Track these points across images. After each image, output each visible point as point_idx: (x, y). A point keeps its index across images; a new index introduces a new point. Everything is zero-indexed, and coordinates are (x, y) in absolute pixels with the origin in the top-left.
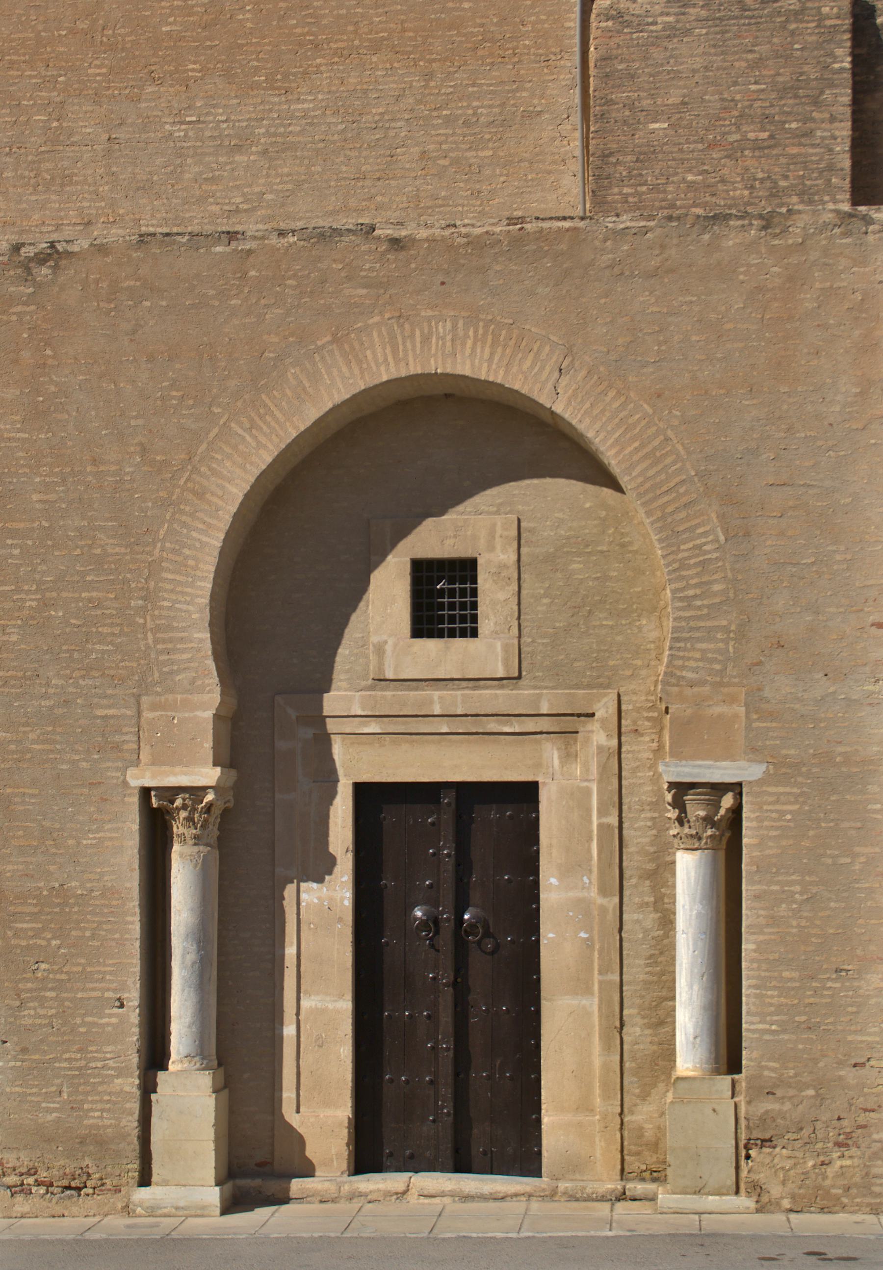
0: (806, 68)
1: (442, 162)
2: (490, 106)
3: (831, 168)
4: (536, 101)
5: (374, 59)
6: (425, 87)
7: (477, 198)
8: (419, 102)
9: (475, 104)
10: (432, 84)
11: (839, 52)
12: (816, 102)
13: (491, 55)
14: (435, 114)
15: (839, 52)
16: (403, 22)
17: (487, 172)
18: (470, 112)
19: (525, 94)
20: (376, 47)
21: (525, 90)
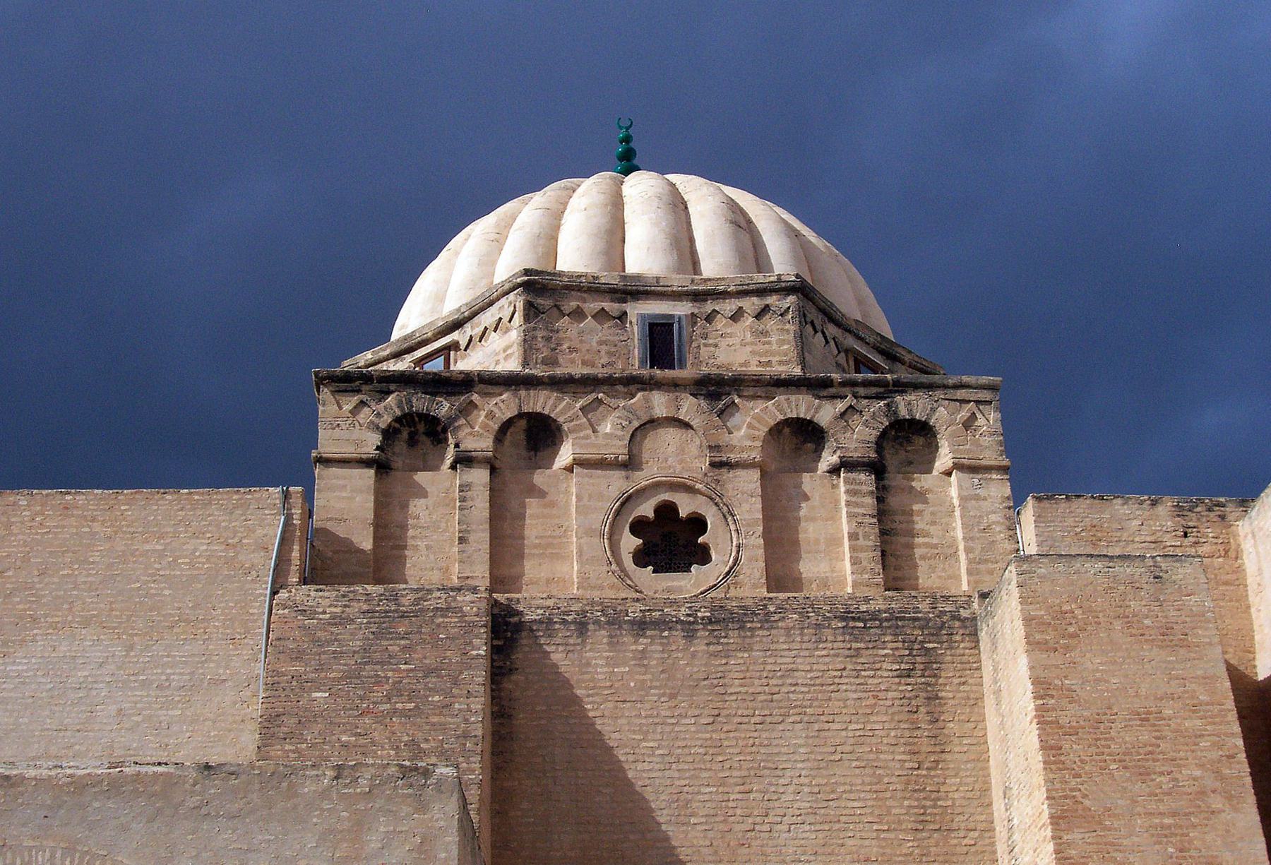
0: (449, 653)
1: (135, 718)
2: (181, 674)
3: (466, 736)
4: (221, 671)
5: (84, 632)
6: (126, 656)
7: (164, 750)
8: (120, 668)
9: (168, 671)
10: (132, 654)
11: (476, 642)
12: (456, 682)
13: (184, 632)
14: (132, 678)
15: (476, 642)
16: (112, 603)
17: (175, 728)
18: (164, 677)
19: (212, 665)
20: (86, 623)
21: (213, 661)
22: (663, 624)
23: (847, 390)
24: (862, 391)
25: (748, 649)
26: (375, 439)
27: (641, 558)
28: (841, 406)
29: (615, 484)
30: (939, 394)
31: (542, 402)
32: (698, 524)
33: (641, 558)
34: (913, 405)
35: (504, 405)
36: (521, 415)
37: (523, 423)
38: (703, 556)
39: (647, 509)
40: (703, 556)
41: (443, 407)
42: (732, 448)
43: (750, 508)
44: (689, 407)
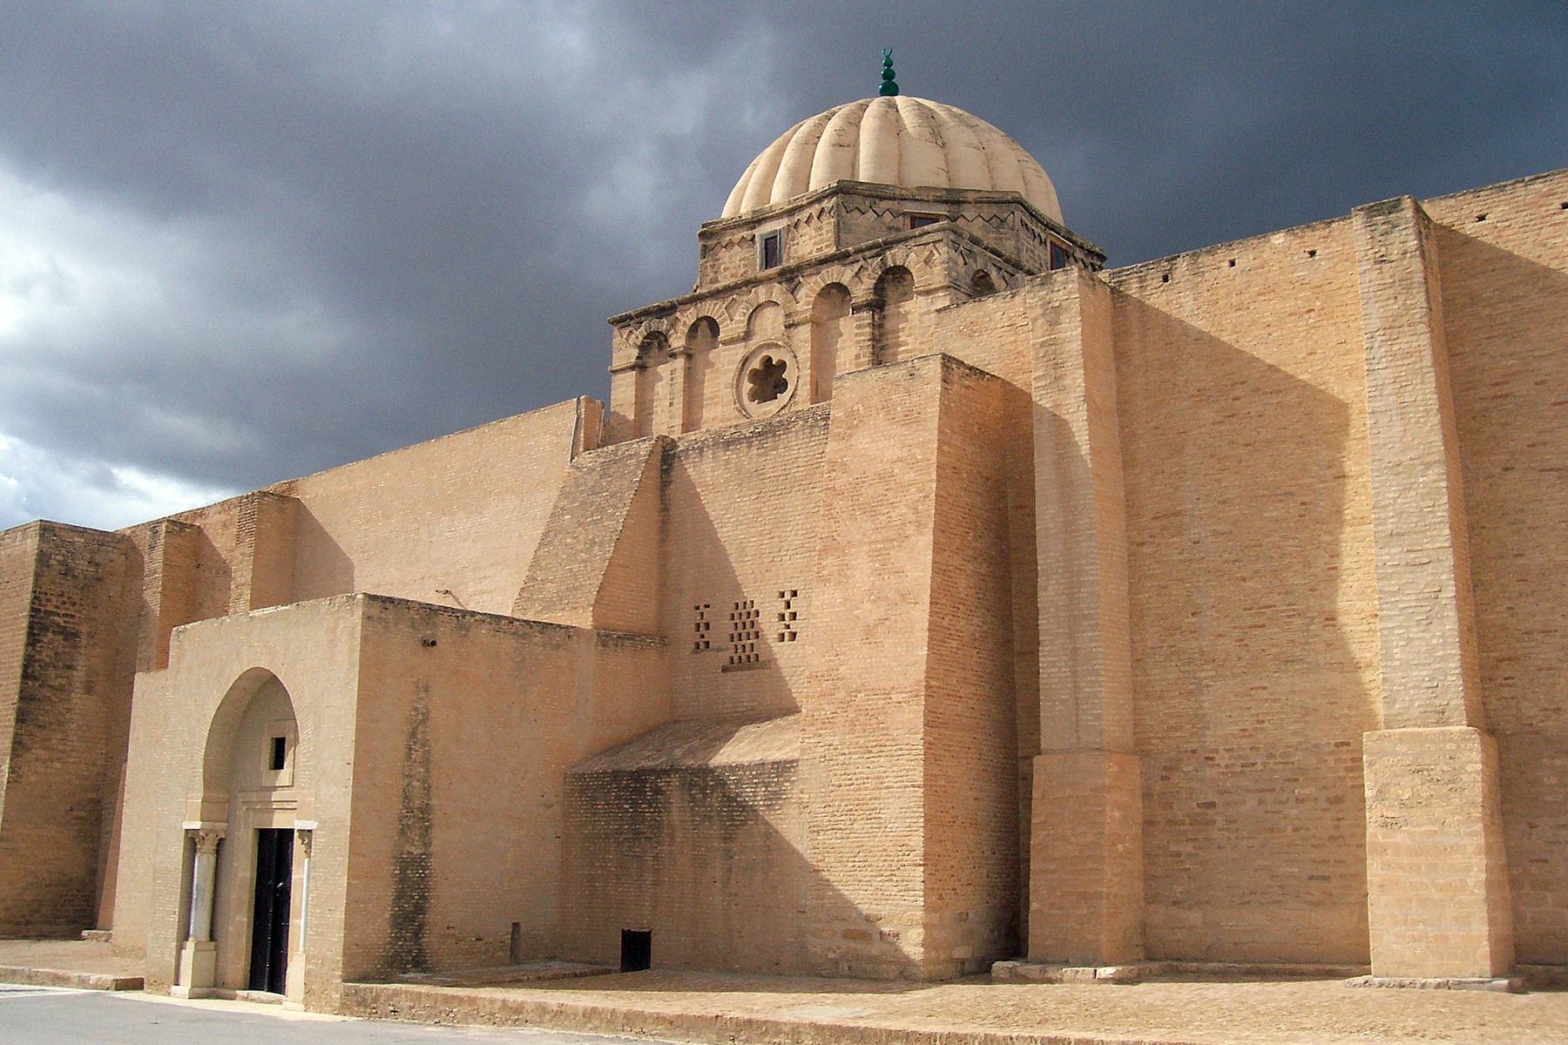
22: (738, 441)
23: (860, 256)
24: (867, 254)
25: (776, 449)
26: (635, 352)
27: (754, 396)
28: (856, 267)
29: (739, 351)
30: (911, 243)
31: (710, 308)
32: (783, 365)
33: (754, 396)
34: (896, 256)
35: (688, 317)
36: (699, 319)
37: (705, 323)
38: (782, 386)
39: (756, 364)
40: (782, 386)
41: (664, 325)
42: (797, 313)
43: (805, 353)
44: (777, 291)
